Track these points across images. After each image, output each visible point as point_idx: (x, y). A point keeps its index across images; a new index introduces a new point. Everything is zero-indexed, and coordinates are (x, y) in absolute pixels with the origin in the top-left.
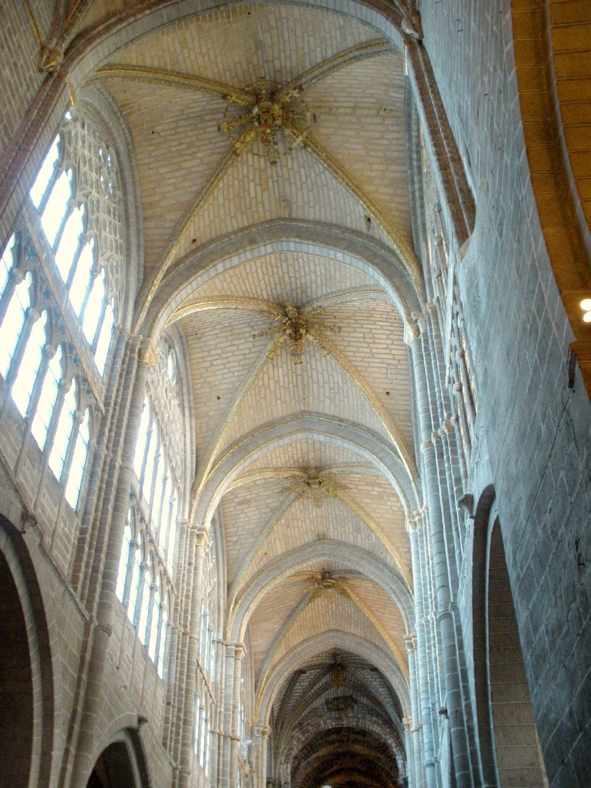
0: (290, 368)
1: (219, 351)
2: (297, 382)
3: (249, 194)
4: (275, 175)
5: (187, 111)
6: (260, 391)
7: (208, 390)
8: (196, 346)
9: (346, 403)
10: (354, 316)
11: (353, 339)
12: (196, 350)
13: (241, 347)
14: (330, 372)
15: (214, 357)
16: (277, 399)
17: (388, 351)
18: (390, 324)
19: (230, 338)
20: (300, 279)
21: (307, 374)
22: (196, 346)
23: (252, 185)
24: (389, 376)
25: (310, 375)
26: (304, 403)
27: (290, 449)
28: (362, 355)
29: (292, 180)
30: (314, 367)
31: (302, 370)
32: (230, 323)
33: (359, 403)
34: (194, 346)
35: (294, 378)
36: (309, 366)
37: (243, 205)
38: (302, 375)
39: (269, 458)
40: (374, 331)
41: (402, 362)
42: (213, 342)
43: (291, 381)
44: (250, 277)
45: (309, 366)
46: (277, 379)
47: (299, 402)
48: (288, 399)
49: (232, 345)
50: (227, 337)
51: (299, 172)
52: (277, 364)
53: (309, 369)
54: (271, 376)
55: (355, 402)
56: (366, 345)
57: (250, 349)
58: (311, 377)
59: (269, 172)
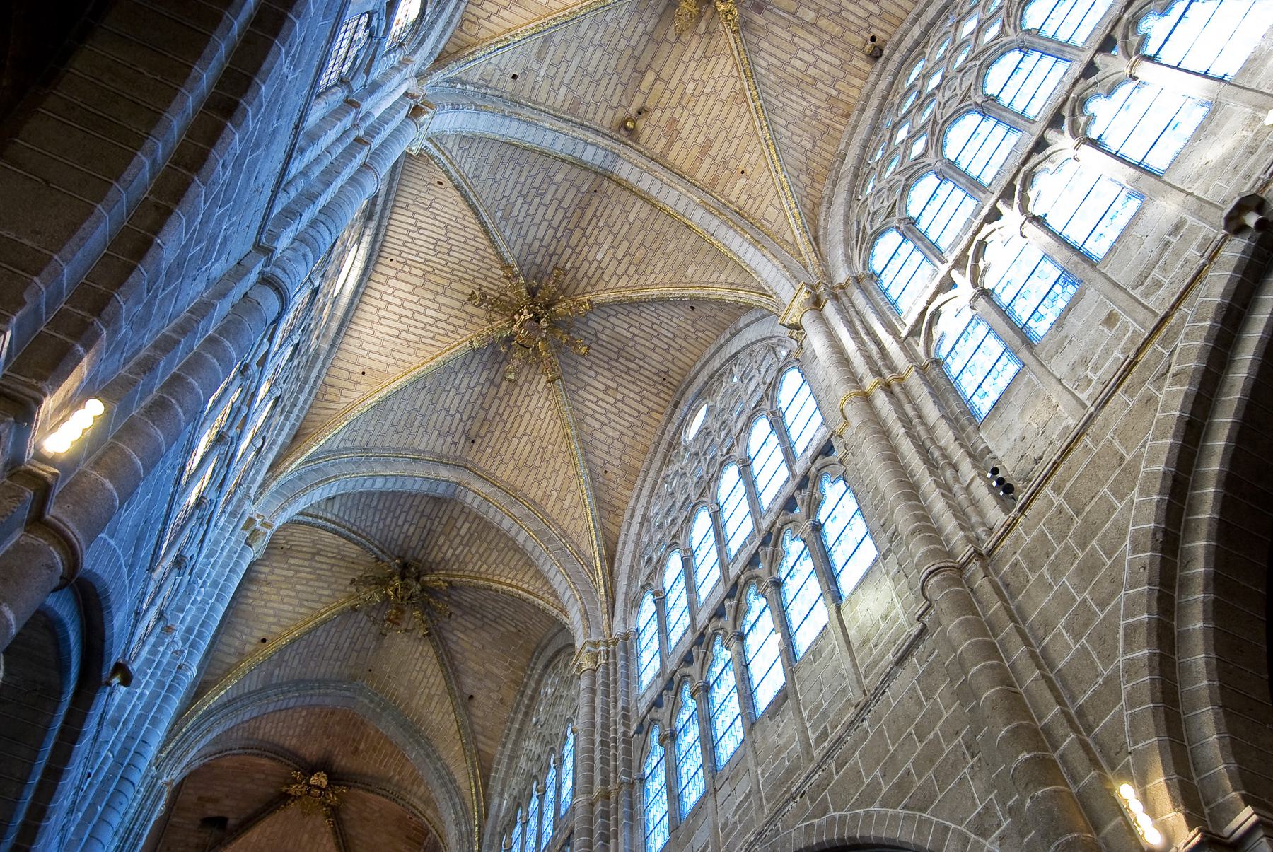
0: (587, 248)
1: (655, 341)
2: (590, 221)
3: (470, 528)
4: (436, 523)
5: (479, 623)
6: (641, 261)
7: (698, 322)
8: (675, 369)
9: (525, 173)
10: (451, 281)
11: (469, 253)
12: (680, 364)
13: (626, 326)
14: (529, 219)
15: (666, 340)
16: (631, 225)
17: (419, 224)
18: (403, 255)
19: (631, 343)
20: (487, 379)
21: (568, 223)
22: (675, 369)
23: (463, 532)
24: (431, 198)
25: (566, 221)
26: (599, 187)
27: (691, 85)
28: (463, 233)
29: (418, 515)
30: (551, 232)
31: (572, 231)
32: (617, 360)
33: (499, 175)
34: (679, 371)
35: (590, 229)
36: (559, 235)
37: (481, 526)
38: (577, 225)
39: (726, 108)
40: (434, 253)
41: (404, 206)
42: (655, 356)
43: (597, 230)
44: (534, 434)
45: (559, 235)
46: (612, 251)
47: (606, 191)
48: (617, 211)
49: (635, 335)
50: (633, 347)
51: (405, 521)
52: (597, 269)
53: (561, 230)
54: (614, 263)
55: (507, 176)
56: (451, 241)
57: (615, 316)
58: (565, 217)
59: (439, 529)
